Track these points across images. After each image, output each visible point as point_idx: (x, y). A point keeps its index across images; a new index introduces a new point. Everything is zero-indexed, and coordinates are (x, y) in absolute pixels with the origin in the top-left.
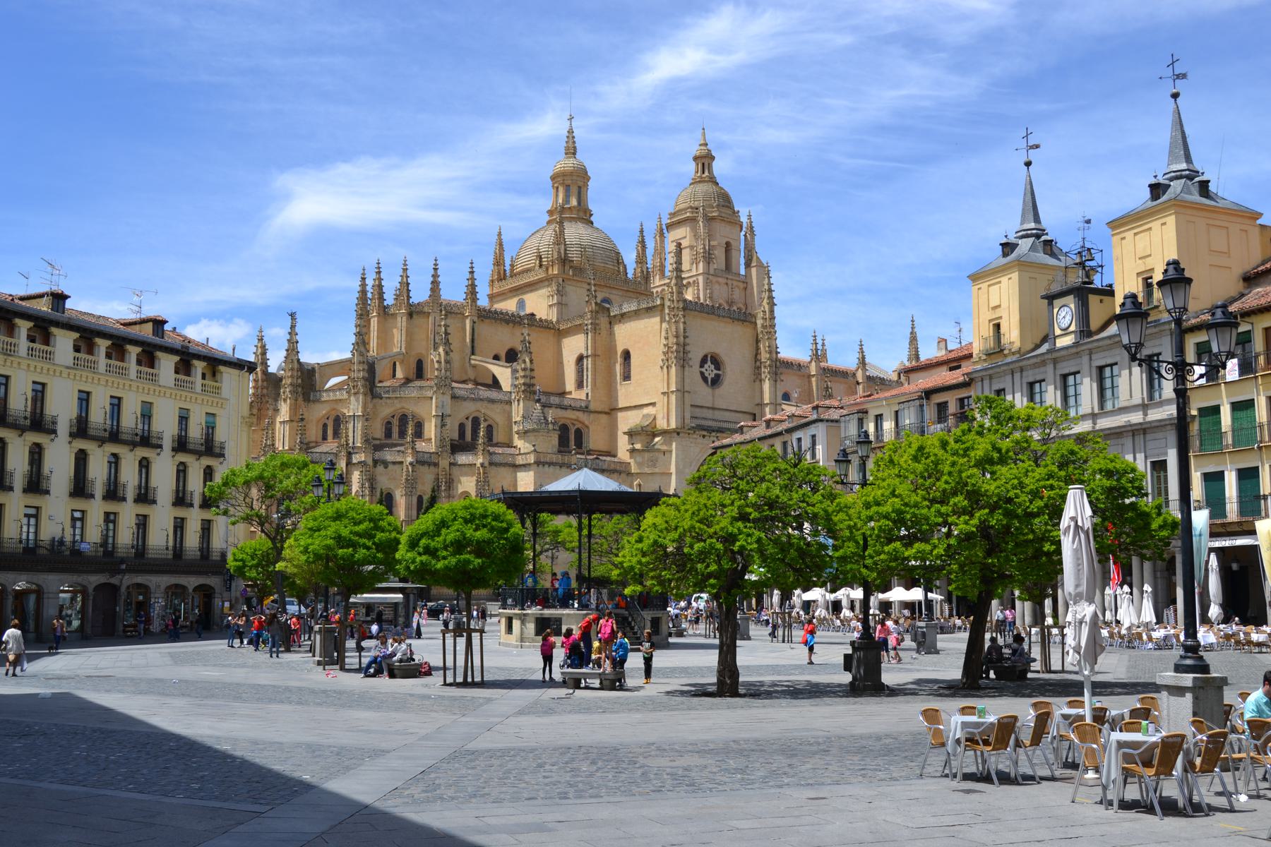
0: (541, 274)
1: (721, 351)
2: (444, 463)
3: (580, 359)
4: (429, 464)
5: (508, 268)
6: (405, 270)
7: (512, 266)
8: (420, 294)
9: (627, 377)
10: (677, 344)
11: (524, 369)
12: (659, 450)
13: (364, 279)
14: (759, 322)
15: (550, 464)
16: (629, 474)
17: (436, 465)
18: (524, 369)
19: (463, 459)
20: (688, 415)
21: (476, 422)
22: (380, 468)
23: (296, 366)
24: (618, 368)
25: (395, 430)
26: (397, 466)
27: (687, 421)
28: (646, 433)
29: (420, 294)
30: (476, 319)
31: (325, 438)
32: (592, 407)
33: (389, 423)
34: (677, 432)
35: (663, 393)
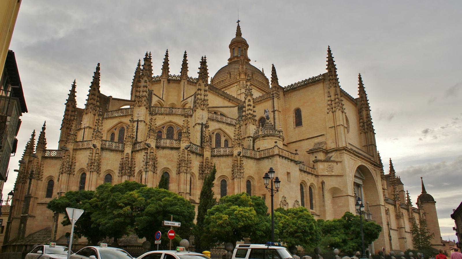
2: (207, 154)
4: (197, 154)
6: (167, 55)
7: (212, 81)
8: (175, 71)
9: (299, 122)
12: (333, 161)
15: (286, 158)
17: (202, 155)
21: (218, 136)
22: (161, 153)
23: (97, 94)
24: (291, 119)
26: (174, 152)
27: (348, 145)
29: (175, 71)
31: (112, 139)
34: (345, 149)
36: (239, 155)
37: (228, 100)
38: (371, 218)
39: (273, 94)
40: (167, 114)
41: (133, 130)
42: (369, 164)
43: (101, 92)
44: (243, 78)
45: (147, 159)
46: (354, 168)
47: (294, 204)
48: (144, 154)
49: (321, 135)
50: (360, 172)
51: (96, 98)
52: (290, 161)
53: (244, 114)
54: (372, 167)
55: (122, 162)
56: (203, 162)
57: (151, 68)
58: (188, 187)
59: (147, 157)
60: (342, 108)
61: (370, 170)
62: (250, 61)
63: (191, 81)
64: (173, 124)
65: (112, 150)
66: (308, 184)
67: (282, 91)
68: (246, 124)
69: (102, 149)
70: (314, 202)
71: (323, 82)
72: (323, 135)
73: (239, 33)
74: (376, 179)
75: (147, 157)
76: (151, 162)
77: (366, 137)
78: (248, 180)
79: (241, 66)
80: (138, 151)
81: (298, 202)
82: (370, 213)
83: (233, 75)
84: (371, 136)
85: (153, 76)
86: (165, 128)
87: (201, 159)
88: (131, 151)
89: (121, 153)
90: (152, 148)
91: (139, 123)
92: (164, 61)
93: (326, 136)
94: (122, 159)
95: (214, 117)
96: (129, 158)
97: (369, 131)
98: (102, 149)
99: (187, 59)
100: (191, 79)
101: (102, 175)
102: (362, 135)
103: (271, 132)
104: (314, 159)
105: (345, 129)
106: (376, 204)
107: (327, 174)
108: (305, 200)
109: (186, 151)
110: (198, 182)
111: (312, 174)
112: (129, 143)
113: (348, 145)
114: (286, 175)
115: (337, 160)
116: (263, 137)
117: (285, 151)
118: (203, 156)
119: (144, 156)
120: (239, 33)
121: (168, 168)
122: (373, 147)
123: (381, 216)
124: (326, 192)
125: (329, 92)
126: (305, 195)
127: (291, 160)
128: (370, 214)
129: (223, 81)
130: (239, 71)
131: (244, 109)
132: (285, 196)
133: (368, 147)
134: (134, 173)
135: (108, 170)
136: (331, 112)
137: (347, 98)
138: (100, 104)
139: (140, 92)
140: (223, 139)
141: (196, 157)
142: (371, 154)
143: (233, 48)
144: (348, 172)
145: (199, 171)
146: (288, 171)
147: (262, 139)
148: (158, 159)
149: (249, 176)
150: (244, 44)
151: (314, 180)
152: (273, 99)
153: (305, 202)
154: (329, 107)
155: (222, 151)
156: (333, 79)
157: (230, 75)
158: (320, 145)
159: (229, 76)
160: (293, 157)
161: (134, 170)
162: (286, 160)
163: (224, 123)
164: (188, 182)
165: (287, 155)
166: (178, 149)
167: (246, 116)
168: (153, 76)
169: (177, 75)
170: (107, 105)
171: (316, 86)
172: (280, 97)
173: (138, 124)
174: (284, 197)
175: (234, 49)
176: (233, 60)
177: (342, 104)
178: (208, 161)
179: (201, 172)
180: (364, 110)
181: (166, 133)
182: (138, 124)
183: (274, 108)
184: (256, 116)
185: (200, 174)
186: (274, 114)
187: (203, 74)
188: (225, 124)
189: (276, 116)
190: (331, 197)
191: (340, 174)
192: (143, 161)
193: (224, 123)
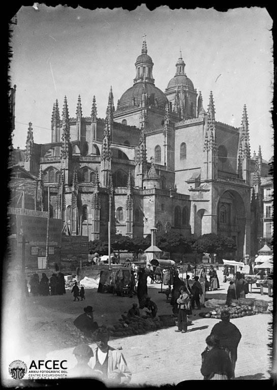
3: (157, 146)
5: (116, 105)
8: (87, 114)
10: (213, 141)
28: (197, 181)
35: (205, 163)
68: (139, 165)
71: (204, 124)
73: (145, 52)
79: (143, 95)
92: (77, 106)
99: (96, 103)
104: (190, 188)
120: (145, 52)
125: (207, 133)
131: (138, 152)
154: (205, 146)
166: (92, 193)
168: (69, 117)
175: (139, 68)
176: (138, 81)
191: (207, 200)
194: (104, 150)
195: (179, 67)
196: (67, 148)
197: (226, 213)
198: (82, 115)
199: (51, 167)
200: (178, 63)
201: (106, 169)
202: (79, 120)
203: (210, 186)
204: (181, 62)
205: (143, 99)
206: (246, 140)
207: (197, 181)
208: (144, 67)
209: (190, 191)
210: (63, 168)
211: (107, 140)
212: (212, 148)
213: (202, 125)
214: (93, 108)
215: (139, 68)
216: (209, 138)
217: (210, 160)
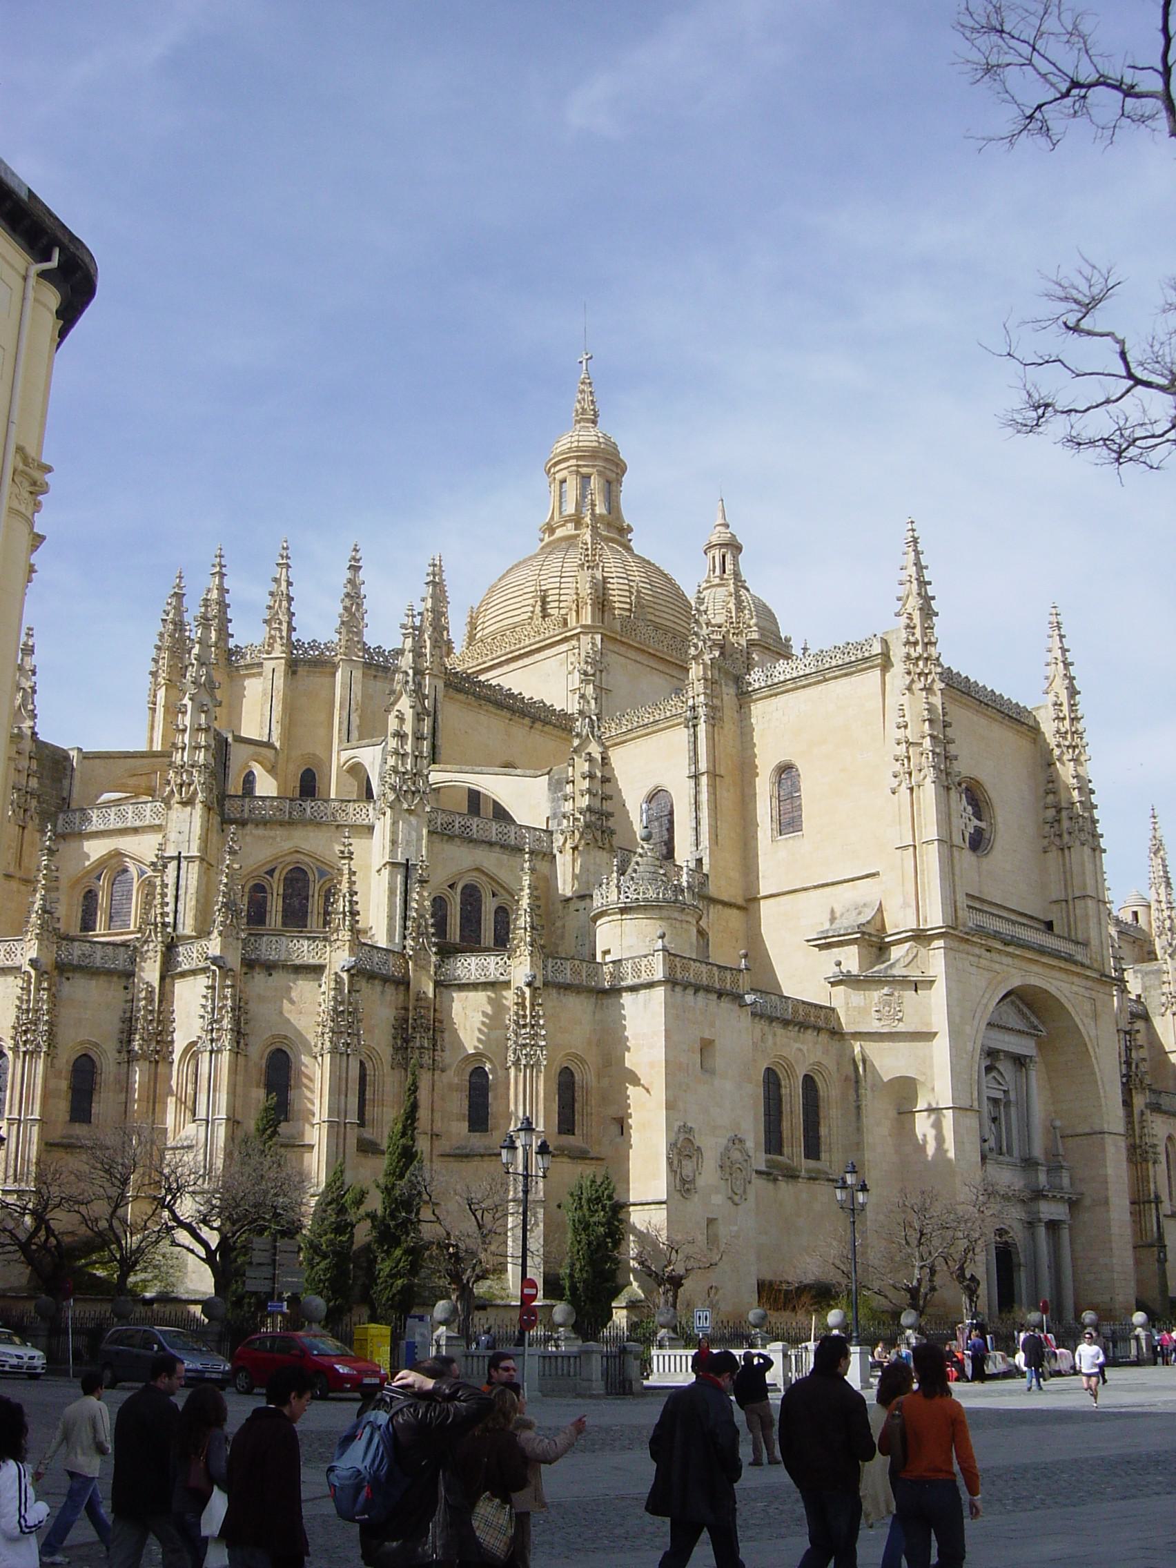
0: (551, 630)
1: (986, 774)
3: (656, 795)
4: (386, 980)
7: (473, 625)
8: (318, 624)
9: (789, 822)
11: (591, 776)
13: (179, 596)
14: (1048, 728)
15: (697, 989)
16: (836, 1033)
17: (403, 983)
18: (591, 776)
19: (470, 967)
20: (962, 901)
21: (471, 896)
23: (27, 745)
25: (275, 907)
27: (963, 914)
30: (440, 684)
32: (713, 890)
33: (259, 888)
36: (529, 985)
37: (527, 721)
38: (1066, 1181)
39: (693, 708)
40: (282, 824)
41: (164, 895)
42: (1063, 976)
43: (41, 737)
44: (589, 622)
45: (213, 1009)
46: (984, 1001)
47: (727, 1149)
48: (204, 991)
49: (867, 876)
50: (1025, 1010)
51: (25, 763)
52: (715, 997)
53: (568, 807)
54: (1075, 988)
55: (128, 1015)
56: (406, 1009)
57: (225, 613)
58: (353, 1101)
59: (213, 1000)
60: (948, 774)
61: (1063, 1000)
62: (630, 530)
63: (378, 666)
64: (307, 859)
65: (91, 972)
66: (801, 1072)
67: (732, 691)
69: (63, 969)
70: (823, 1131)
72: (873, 875)
74: (1093, 1033)
75: (213, 1000)
76: (225, 1021)
77: (1064, 865)
78: (567, 1068)
80: (183, 975)
81: (741, 1141)
82: (1064, 1164)
83: (556, 604)
84: (1083, 864)
85: (232, 643)
86: (276, 874)
87: (401, 997)
88: (157, 975)
89: (123, 982)
90: (231, 970)
91: (184, 864)
93: (882, 877)
94: (127, 1001)
95: (457, 825)
96: (153, 1000)
97: (1078, 843)
98: (63, 969)
99: (362, 575)
100: (378, 654)
101: (65, 1059)
102: (1050, 855)
103: (651, 894)
105: (956, 853)
106: (1087, 1130)
107: (875, 1026)
108: (785, 1125)
109: (345, 976)
110: (388, 1080)
111: (819, 1030)
112: (152, 945)
113: (963, 914)
114: (697, 1047)
115: (914, 973)
116: (623, 911)
117: (698, 964)
118: (408, 984)
119: (205, 997)
121: (286, 1037)
122: (1086, 907)
123: (1106, 1176)
124: (869, 1093)
126: (786, 1107)
127: (720, 995)
128: (1062, 1167)
129: (514, 627)
130: (577, 594)
131: (569, 788)
132: (689, 1124)
133: (1070, 902)
134: (172, 1053)
135: (81, 1043)
136: (904, 790)
137: (990, 711)
138: (39, 783)
139: (183, 749)
140: (489, 906)
141: (383, 992)
142: (1080, 938)
143: (559, 476)
144: (957, 1020)
145: (394, 1038)
146: (707, 1036)
147: (619, 917)
148: (252, 1007)
149: (568, 1055)
150: (606, 460)
151: (826, 1052)
152: (695, 726)
153: (785, 1136)
155: (473, 967)
156: (918, 659)
157: (544, 603)
158: (859, 913)
159: (538, 609)
160: (729, 981)
161: (172, 1042)
162: (701, 994)
163: (491, 844)
164: (350, 1085)
165: (705, 975)
167: (576, 819)
168: (232, 643)
169: (322, 640)
170: (66, 782)
171: (853, 679)
172: (721, 719)
173: (179, 868)
174: (686, 1130)
175: (563, 481)
176: (560, 533)
177: (946, 758)
178: (423, 1004)
179: (399, 1042)
180: (1065, 757)
181: (281, 892)
182: (179, 868)
183: (696, 762)
184: (611, 815)
185: (396, 1049)
186: (697, 785)
187: (411, 672)
188: (497, 849)
189: (704, 797)
190: (893, 1113)
192: (202, 1017)
193: (491, 844)
194: (391, 761)
195: (717, 553)
196: (197, 747)
197: (1007, 1104)
198: (291, 629)
199: (118, 854)
200: (715, 539)
201: (400, 859)
202: (278, 651)
203: (935, 961)
204: (726, 537)
205: (586, 590)
206: (1076, 760)
207: (875, 942)
208: (586, 478)
209: (833, 984)
210: (171, 852)
211: (409, 714)
212: (931, 774)
213: (878, 672)
214: (348, 595)
215: (563, 481)
216: (919, 730)
217: (930, 830)
